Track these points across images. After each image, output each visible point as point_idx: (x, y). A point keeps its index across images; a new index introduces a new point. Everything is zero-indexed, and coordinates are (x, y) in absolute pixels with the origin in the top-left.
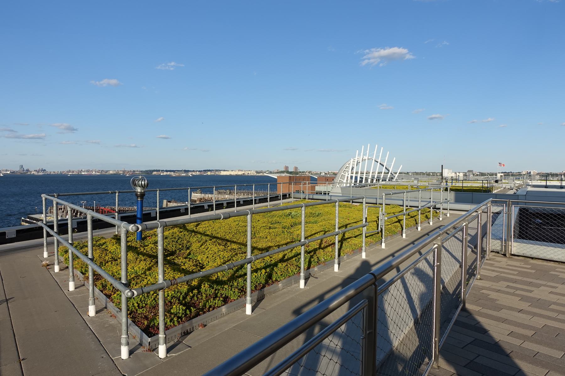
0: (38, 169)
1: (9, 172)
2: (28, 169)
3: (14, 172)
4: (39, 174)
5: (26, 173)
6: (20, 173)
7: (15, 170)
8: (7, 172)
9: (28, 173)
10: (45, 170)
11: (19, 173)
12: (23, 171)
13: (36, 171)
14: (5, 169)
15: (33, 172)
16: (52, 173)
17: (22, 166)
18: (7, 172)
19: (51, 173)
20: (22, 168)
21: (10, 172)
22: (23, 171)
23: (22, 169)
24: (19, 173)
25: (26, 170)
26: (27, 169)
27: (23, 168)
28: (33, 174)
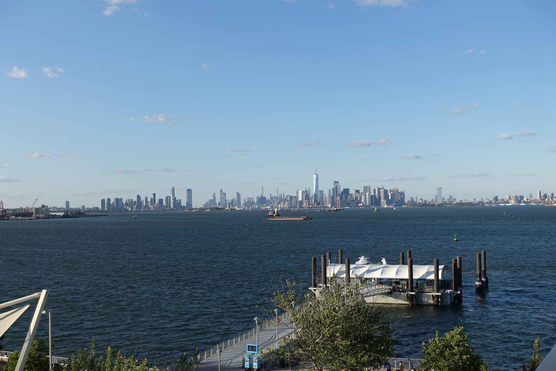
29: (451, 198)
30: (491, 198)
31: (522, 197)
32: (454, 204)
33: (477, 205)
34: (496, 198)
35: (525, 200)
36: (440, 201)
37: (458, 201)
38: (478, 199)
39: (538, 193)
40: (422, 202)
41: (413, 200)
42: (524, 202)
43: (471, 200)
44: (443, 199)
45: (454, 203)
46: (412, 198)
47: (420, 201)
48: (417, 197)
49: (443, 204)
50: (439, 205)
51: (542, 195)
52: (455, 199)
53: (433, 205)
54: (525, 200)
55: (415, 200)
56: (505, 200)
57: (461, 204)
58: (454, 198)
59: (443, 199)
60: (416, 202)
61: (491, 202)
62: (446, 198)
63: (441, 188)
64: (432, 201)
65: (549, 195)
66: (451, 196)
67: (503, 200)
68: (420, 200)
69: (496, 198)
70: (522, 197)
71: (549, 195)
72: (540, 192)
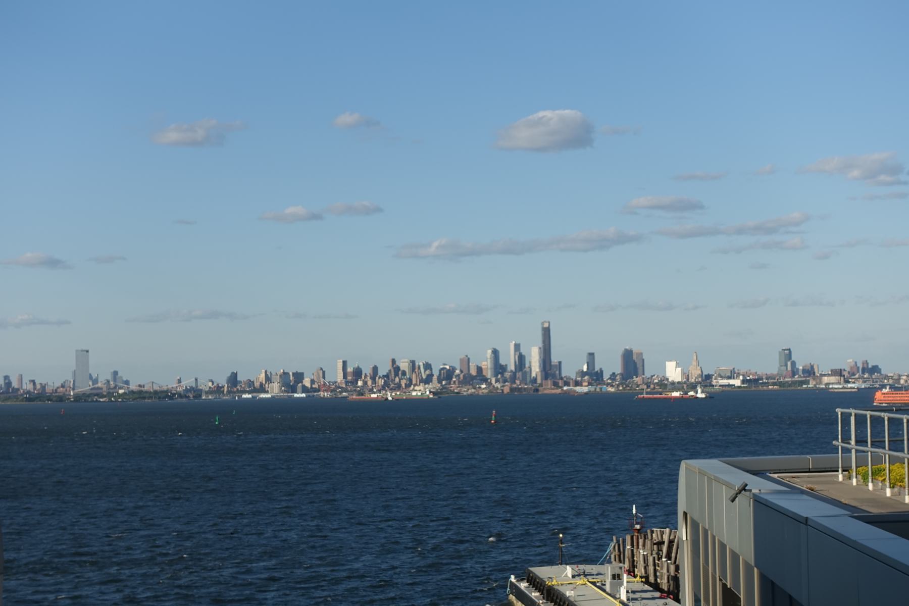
0: (846, 364)
1: (737, 382)
2: (812, 367)
3: (755, 381)
4: (849, 385)
5: (802, 383)
6: (781, 384)
7: (765, 372)
8: (732, 382)
9: (807, 382)
10: (875, 369)
11: (774, 384)
12: (794, 372)
13: (838, 373)
14: (726, 367)
15: (826, 379)
16: (902, 382)
17: (788, 355)
18: (732, 382)
19: (899, 379)
20: (789, 364)
21: (743, 382)
22: (794, 372)
23: (789, 368)
24: (774, 384)
25: (804, 371)
26: (809, 368)
27: (793, 364)
28: (826, 391)
29: (115, 380)
30: (222, 381)
31: (299, 377)
32: (120, 396)
33: (180, 396)
34: (233, 379)
35: (307, 383)
36: (85, 387)
37: (133, 387)
38: (188, 382)
39: (340, 365)
40: (35, 389)
41: (8, 384)
42: (305, 389)
43: (166, 381)
44: (95, 381)
45: (121, 391)
46: (6, 377)
47: (30, 387)
48: (21, 375)
49: (89, 396)
50: (78, 398)
51: (350, 369)
52: (127, 382)
53: (61, 399)
54: (307, 383)
55: (15, 384)
56: (257, 385)
57: (140, 394)
58: (125, 379)
59: (95, 381)
60: (18, 390)
61: (218, 390)
62: (104, 377)
63: (87, 351)
64: (63, 386)
65: (367, 370)
66: (115, 373)
67: (250, 383)
68: (28, 382)
69: (233, 379)
70: (299, 377)
71: (367, 370)
72: (345, 363)
